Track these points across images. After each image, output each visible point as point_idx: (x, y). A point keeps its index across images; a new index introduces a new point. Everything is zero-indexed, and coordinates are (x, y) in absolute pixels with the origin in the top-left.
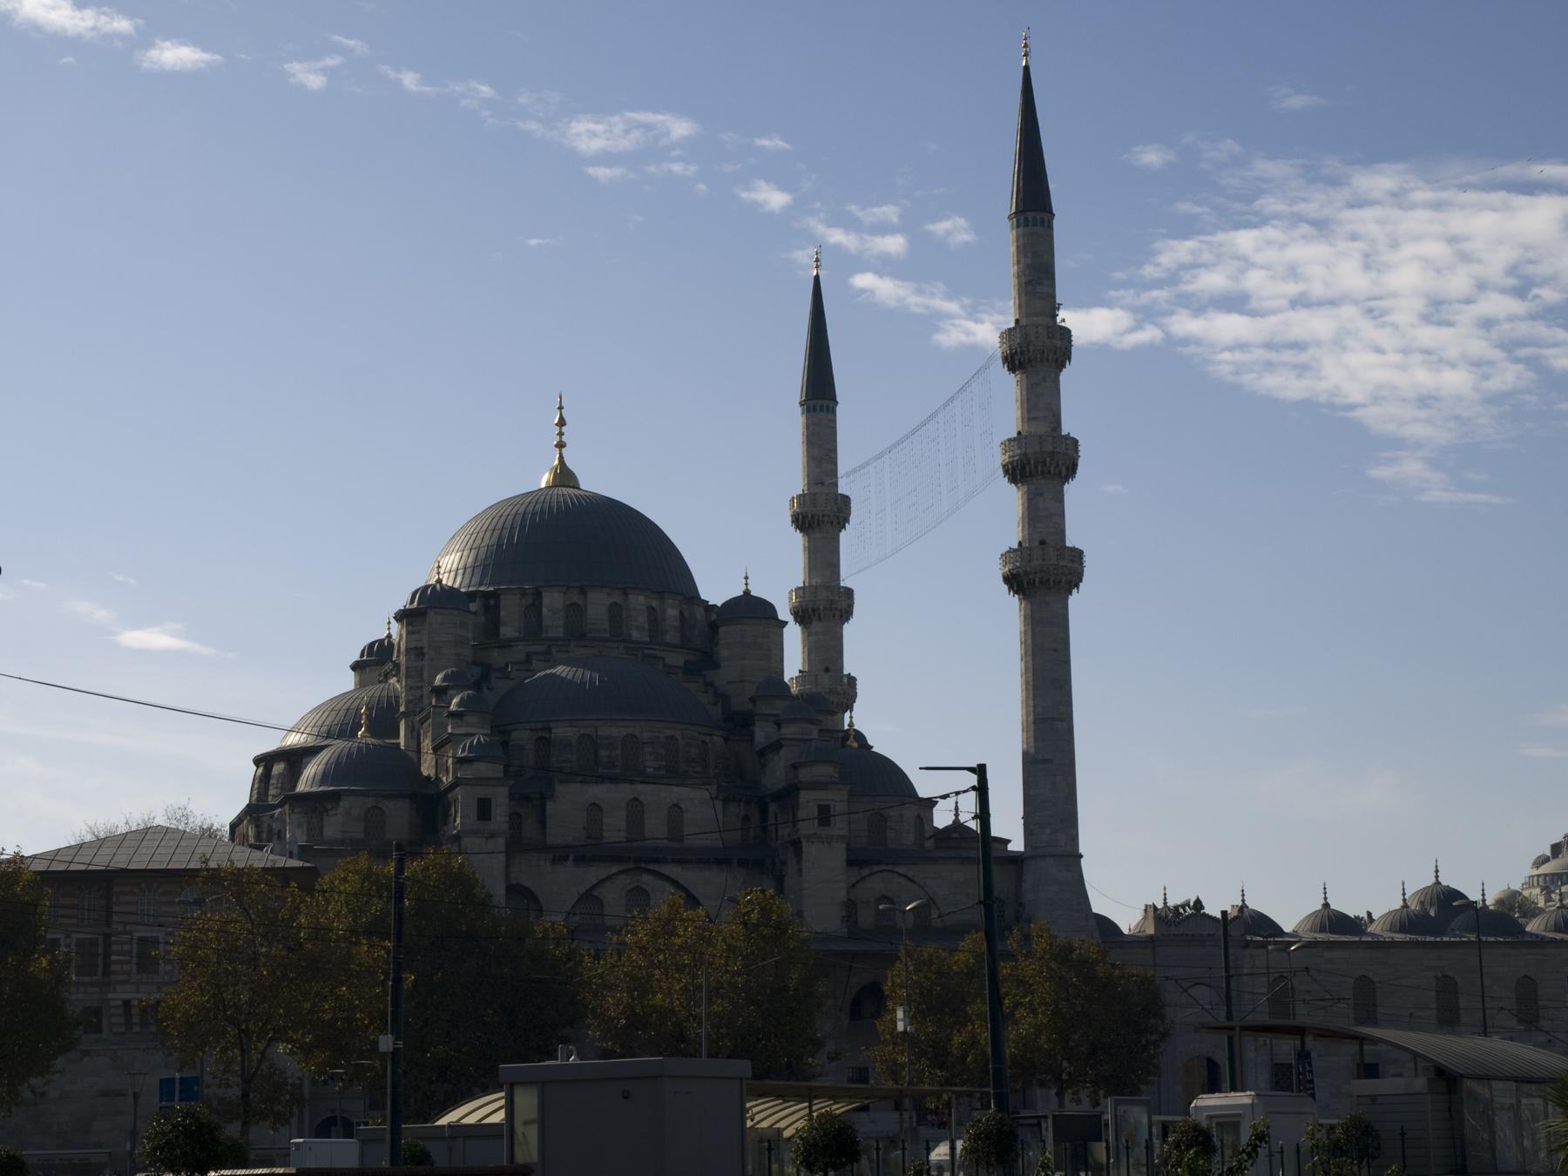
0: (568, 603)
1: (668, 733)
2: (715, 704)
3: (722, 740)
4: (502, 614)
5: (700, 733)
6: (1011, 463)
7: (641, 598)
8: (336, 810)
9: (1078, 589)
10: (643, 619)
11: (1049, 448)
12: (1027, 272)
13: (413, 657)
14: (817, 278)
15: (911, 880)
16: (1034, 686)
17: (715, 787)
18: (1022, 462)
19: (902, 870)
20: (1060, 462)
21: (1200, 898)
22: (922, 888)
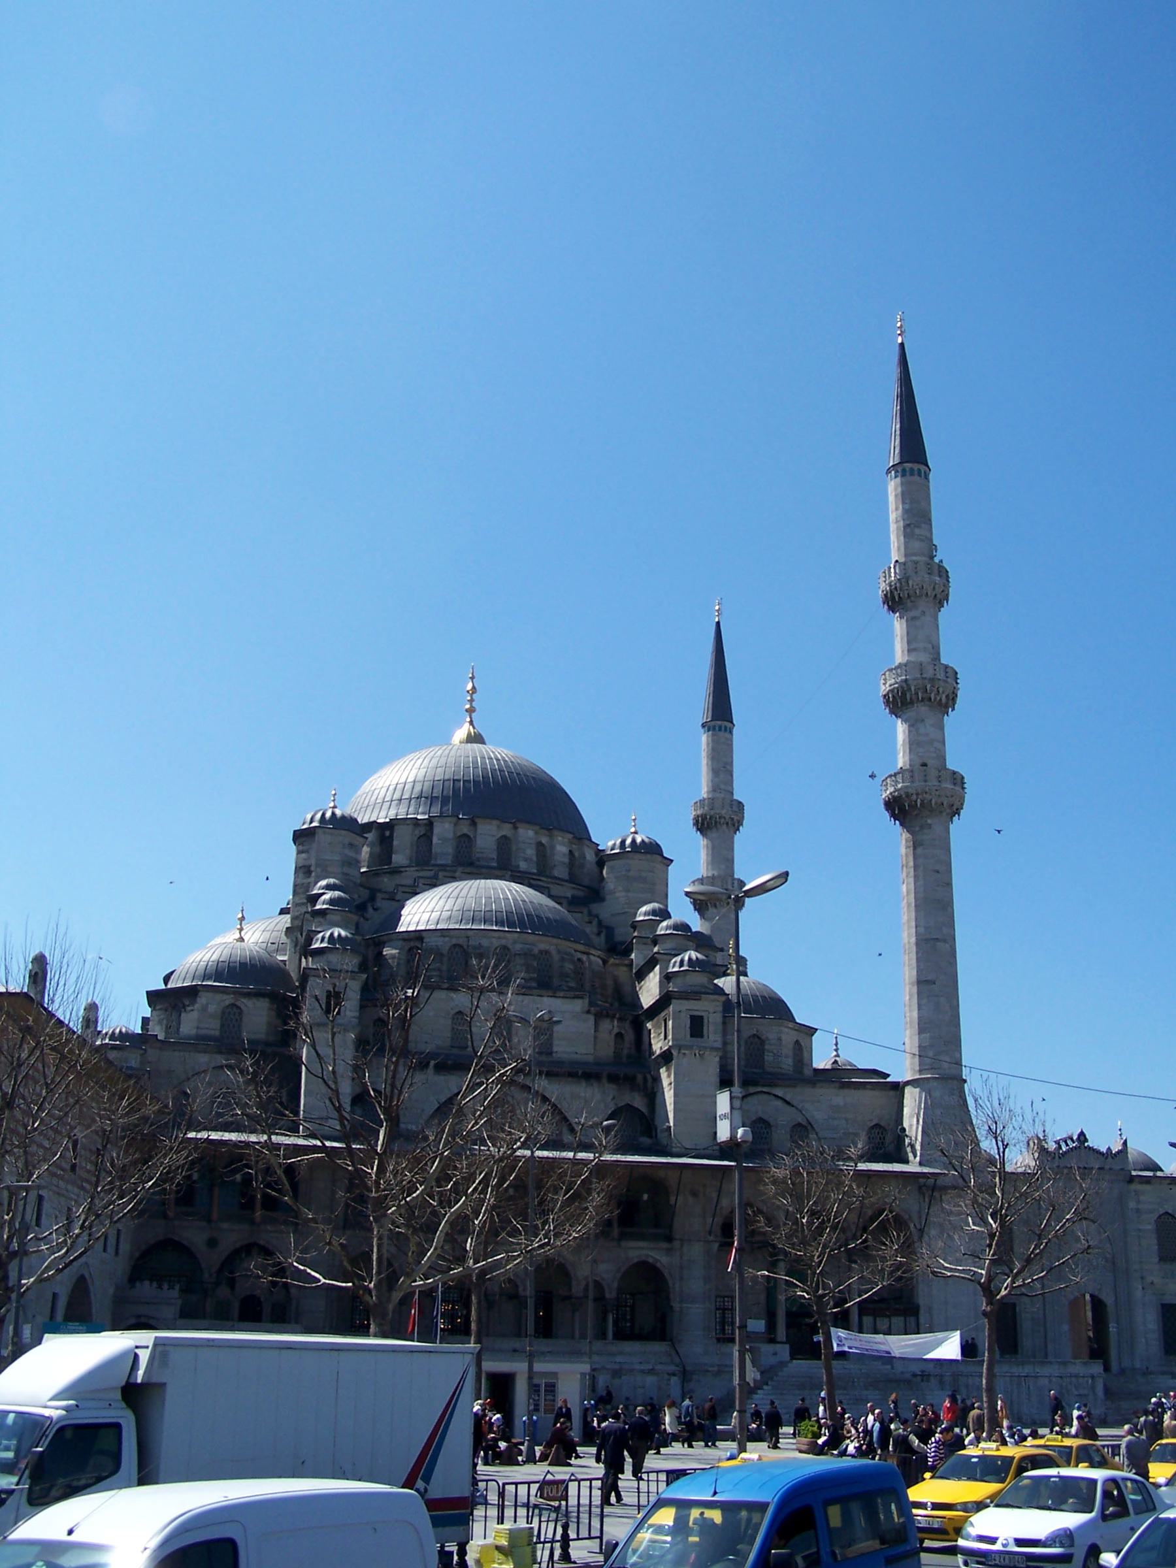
0: (459, 834)
1: (543, 946)
2: (599, 934)
3: (600, 962)
4: (395, 843)
5: (576, 951)
6: (891, 691)
7: (531, 833)
8: (193, 1006)
9: (959, 815)
10: (531, 852)
11: (929, 673)
12: (906, 516)
13: (301, 875)
14: (718, 623)
15: (788, 1103)
16: (916, 906)
17: (587, 1001)
18: (902, 687)
19: (779, 1092)
20: (941, 690)
21: (1084, 1131)
22: (801, 1111)
